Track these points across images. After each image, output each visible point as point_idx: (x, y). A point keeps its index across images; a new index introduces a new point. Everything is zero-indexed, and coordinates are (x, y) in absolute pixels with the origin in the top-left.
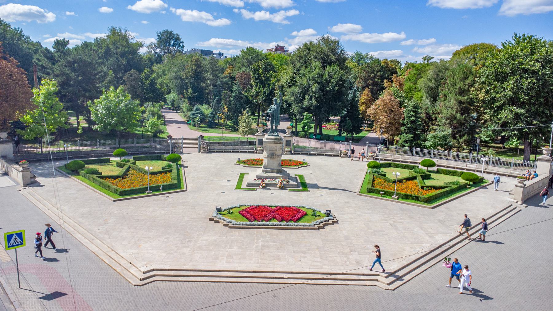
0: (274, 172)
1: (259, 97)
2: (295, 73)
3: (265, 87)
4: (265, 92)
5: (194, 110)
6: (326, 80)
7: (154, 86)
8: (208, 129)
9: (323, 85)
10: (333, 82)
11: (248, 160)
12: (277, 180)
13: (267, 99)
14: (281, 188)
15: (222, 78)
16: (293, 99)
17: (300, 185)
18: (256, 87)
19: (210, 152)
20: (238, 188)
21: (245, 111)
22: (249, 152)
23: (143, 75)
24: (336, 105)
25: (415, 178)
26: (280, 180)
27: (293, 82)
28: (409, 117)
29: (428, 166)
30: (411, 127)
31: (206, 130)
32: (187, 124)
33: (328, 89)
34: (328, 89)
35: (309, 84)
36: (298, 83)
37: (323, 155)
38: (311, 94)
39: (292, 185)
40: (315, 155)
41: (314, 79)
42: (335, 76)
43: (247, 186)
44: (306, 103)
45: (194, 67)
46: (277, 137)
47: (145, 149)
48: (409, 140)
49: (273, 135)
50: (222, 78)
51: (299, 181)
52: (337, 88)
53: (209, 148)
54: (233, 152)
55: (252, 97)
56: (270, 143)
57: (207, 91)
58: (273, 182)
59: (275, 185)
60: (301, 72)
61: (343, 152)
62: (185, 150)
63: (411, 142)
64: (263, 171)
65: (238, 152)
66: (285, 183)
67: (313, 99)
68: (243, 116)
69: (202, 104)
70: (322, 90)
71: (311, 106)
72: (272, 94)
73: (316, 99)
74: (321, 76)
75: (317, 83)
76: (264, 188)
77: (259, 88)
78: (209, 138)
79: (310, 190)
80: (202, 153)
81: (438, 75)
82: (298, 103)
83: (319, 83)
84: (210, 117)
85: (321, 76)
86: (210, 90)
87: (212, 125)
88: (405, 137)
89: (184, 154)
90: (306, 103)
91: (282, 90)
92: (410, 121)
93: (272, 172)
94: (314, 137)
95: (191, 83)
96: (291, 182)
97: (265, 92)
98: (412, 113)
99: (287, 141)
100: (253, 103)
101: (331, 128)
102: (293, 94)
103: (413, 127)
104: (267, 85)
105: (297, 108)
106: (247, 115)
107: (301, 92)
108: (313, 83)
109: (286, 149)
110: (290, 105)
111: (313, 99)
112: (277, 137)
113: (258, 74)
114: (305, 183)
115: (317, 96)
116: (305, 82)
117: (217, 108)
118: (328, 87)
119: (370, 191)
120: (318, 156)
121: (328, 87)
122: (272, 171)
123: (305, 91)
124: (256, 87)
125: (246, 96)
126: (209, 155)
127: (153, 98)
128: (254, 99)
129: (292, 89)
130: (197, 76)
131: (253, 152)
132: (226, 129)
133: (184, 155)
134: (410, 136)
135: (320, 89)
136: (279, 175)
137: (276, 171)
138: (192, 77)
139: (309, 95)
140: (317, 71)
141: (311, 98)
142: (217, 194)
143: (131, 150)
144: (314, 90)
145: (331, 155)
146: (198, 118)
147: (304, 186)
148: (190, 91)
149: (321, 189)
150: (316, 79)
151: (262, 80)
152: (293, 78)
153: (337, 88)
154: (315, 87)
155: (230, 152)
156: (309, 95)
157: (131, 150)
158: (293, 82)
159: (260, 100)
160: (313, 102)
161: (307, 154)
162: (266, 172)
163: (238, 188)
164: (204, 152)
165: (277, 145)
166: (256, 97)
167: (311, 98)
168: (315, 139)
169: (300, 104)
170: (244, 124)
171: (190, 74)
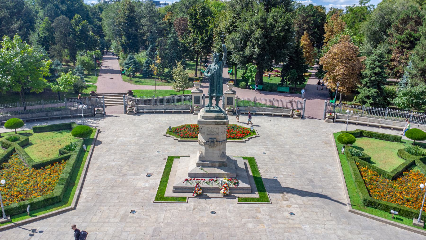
0: (215, 167)
1: (196, 44)
2: (234, 17)
4: (202, 39)
5: (128, 59)
6: (271, 24)
7: (85, 33)
8: (142, 80)
9: (267, 31)
10: (279, 26)
11: (182, 127)
12: (220, 180)
13: (205, 47)
14: (226, 196)
15: (160, 24)
16: (233, 46)
17: (254, 185)
18: (194, 33)
19: (138, 113)
20: (160, 197)
21: (180, 63)
22: (184, 112)
23: (73, 21)
24: (280, 53)
25: (413, 164)
26: (224, 180)
28: (373, 69)
30: (374, 80)
31: (140, 82)
32: (122, 74)
33: (272, 34)
34: (272, 34)
35: (251, 30)
36: (239, 29)
37: (271, 115)
38: (253, 41)
39: (243, 189)
40: (261, 115)
41: (257, 23)
42: (281, 20)
43: (174, 192)
44: (248, 51)
45: (127, 12)
46: (220, 114)
47: (57, 113)
49: (212, 111)
50: (160, 24)
51: (251, 174)
52: (282, 34)
53: (138, 107)
54: (166, 112)
55: (189, 44)
56: (208, 123)
57: (145, 38)
58: (214, 185)
59: (217, 190)
60: (242, 16)
61: (295, 112)
62: (108, 110)
63: (375, 98)
64: (198, 165)
65: (171, 112)
66: (232, 186)
67: (256, 46)
69: (137, 51)
70: (265, 36)
71: (253, 54)
72: (209, 41)
73: (259, 45)
74: (264, 20)
75: (261, 28)
76: (199, 196)
78: (142, 92)
79: (272, 196)
80: (128, 114)
81: (383, 18)
82: (239, 51)
83: (262, 29)
84: (145, 66)
85: (264, 20)
86: (147, 36)
87: (148, 75)
88: (366, 92)
89: (107, 116)
90: (248, 51)
92: (374, 74)
93: (212, 166)
95: (124, 30)
96: (242, 185)
98: (377, 63)
99: (228, 99)
100: (191, 51)
101: (272, 77)
102: (233, 41)
103: (377, 80)
104: (204, 31)
105: (237, 57)
106: (182, 67)
107: (242, 38)
109: (227, 109)
111: (256, 46)
112: (220, 114)
113: (195, 19)
114: (260, 178)
115: (260, 43)
116: (246, 28)
117: (152, 55)
119: (369, 204)
120: (266, 117)
121: (273, 32)
122: (213, 165)
123: (247, 37)
124: (194, 33)
125: (182, 44)
126: (136, 117)
127: (84, 46)
128: (191, 47)
129: (232, 35)
130: (130, 21)
131: (188, 112)
132: (162, 79)
133: (106, 119)
134: (373, 91)
135: (264, 35)
136: (222, 172)
137: (217, 164)
138: (126, 23)
139: (251, 42)
140: (261, 14)
141: (253, 45)
142: (123, 219)
143: (39, 114)
144: (256, 36)
145: (280, 116)
146: (131, 68)
147: (262, 188)
148: (124, 38)
149: (287, 195)
150: (260, 24)
151: (200, 26)
152: (233, 23)
153: (282, 34)
154: (258, 33)
155: (161, 113)
156: (251, 42)
157: (39, 114)
159: (197, 47)
160: (256, 50)
162: (204, 166)
163: (160, 197)
164: (132, 113)
165: (219, 126)
166: (194, 44)
167: (253, 45)
168: (257, 90)
169: (241, 53)
170: (178, 78)
171: (122, 20)
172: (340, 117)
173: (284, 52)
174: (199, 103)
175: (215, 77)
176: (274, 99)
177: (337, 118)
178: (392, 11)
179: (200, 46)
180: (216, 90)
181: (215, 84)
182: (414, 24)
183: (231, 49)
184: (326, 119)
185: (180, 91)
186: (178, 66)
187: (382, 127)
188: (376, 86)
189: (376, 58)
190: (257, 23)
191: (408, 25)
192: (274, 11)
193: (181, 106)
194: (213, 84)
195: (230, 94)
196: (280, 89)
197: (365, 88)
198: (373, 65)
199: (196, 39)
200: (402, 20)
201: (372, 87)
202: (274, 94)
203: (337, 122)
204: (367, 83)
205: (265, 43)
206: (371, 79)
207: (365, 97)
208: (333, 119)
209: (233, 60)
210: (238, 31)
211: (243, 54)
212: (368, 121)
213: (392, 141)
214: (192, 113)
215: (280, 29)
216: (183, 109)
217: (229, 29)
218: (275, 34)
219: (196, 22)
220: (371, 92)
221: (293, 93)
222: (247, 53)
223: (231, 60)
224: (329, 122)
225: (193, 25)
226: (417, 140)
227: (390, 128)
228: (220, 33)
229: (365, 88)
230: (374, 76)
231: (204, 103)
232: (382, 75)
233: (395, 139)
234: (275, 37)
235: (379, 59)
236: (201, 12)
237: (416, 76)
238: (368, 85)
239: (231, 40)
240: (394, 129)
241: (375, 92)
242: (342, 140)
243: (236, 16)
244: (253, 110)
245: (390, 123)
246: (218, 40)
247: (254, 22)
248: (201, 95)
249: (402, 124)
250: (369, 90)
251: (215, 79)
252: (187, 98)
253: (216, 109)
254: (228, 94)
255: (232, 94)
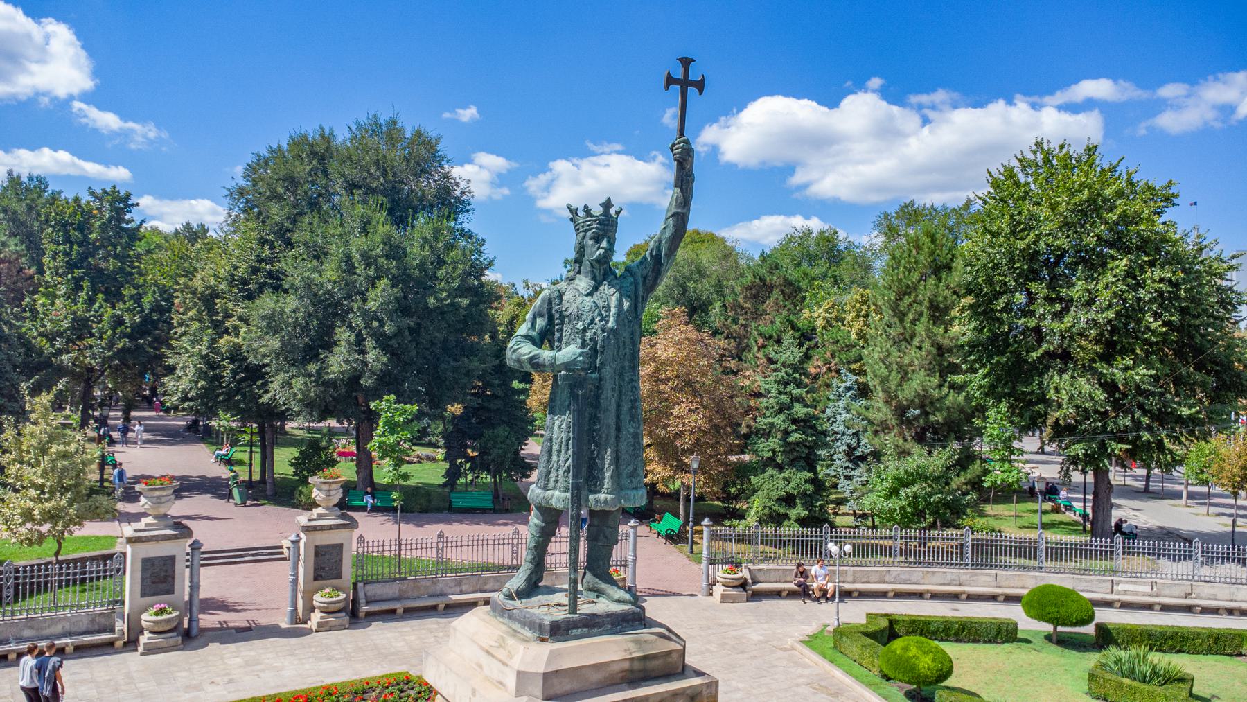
1: (91, 341)
3: (121, 298)
4: (119, 321)
6: (422, 267)
9: (415, 286)
16: (275, 343)
21: (45, 399)
24: (456, 369)
27: (260, 278)
29: (1056, 622)
30: (797, 444)
34: (432, 301)
41: (369, 261)
44: (337, 362)
48: (804, 495)
49: (593, 625)
52: (465, 302)
67: (369, 343)
68: (28, 428)
70: (402, 309)
73: (383, 342)
77: (91, 301)
81: (685, 290)
82: (305, 362)
85: (395, 252)
88: (780, 483)
90: (337, 362)
91: (211, 311)
94: (369, 500)
97: (119, 321)
99: (320, 552)
102: (273, 324)
104: (127, 291)
105: (298, 383)
108: (373, 282)
109: (318, 599)
110: (256, 374)
111: (369, 343)
115: (388, 329)
118: (434, 294)
121: (434, 294)
123: (328, 312)
128: (59, 352)
129: (267, 302)
134: (798, 479)
141: (360, 340)
144: (372, 305)
151: (100, 271)
152: (261, 261)
153: (465, 302)
154: (380, 295)
158: (260, 278)
159: (93, 353)
161: (431, 611)
167: (360, 340)
168: (375, 509)
169: (312, 368)
170: (33, 475)
172: (760, 577)
173: (471, 366)
174: (170, 591)
175: (607, 372)
176: (441, 535)
177: (754, 582)
178: (701, 273)
179: (110, 348)
180: (617, 460)
181: (609, 419)
182: (781, 297)
183: (264, 356)
184: (718, 590)
185: (42, 538)
186: (33, 416)
187: (899, 595)
188: (803, 463)
189: (788, 375)
190: (369, 261)
191: (770, 303)
192: (423, 224)
193: (60, 620)
194: (594, 418)
195: (331, 528)
196: (458, 503)
197: (770, 471)
198: (782, 397)
199: (87, 319)
200: (749, 288)
201: (791, 465)
202: (448, 521)
203: (757, 596)
204: (773, 451)
205: (407, 333)
206: (791, 439)
207: (780, 500)
208: (743, 585)
209: (274, 399)
210: (292, 286)
211: (319, 372)
212: (850, 579)
213: (990, 642)
214: (131, 644)
215: (455, 285)
216: (70, 634)
217: (245, 282)
218: (440, 300)
219: (84, 257)
220: (793, 484)
221: (507, 511)
222: (336, 369)
223: (265, 398)
224: (734, 600)
225: (71, 266)
226: (1063, 625)
227: (919, 595)
228: (209, 299)
229: (770, 471)
230: (795, 431)
231: (195, 587)
232: (813, 427)
233: (999, 632)
234: (441, 311)
235: (797, 375)
236: (110, 220)
237: (884, 427)
238: (779, 460)
239: (264, 318)
240: (935, 596)
241: (806, 481)
242: (913, 668)
243: (271, 237)
244: (432, 590)
245: (914, 578)
246: (196, 325)
247: (355, 256)
248: (180, 549)
249: (949, 577)
250: (786, 474)
251: (608, 385)
252: (95, 570)
253: (604, 606)
254: (323, 528)
255: (338, 527)
